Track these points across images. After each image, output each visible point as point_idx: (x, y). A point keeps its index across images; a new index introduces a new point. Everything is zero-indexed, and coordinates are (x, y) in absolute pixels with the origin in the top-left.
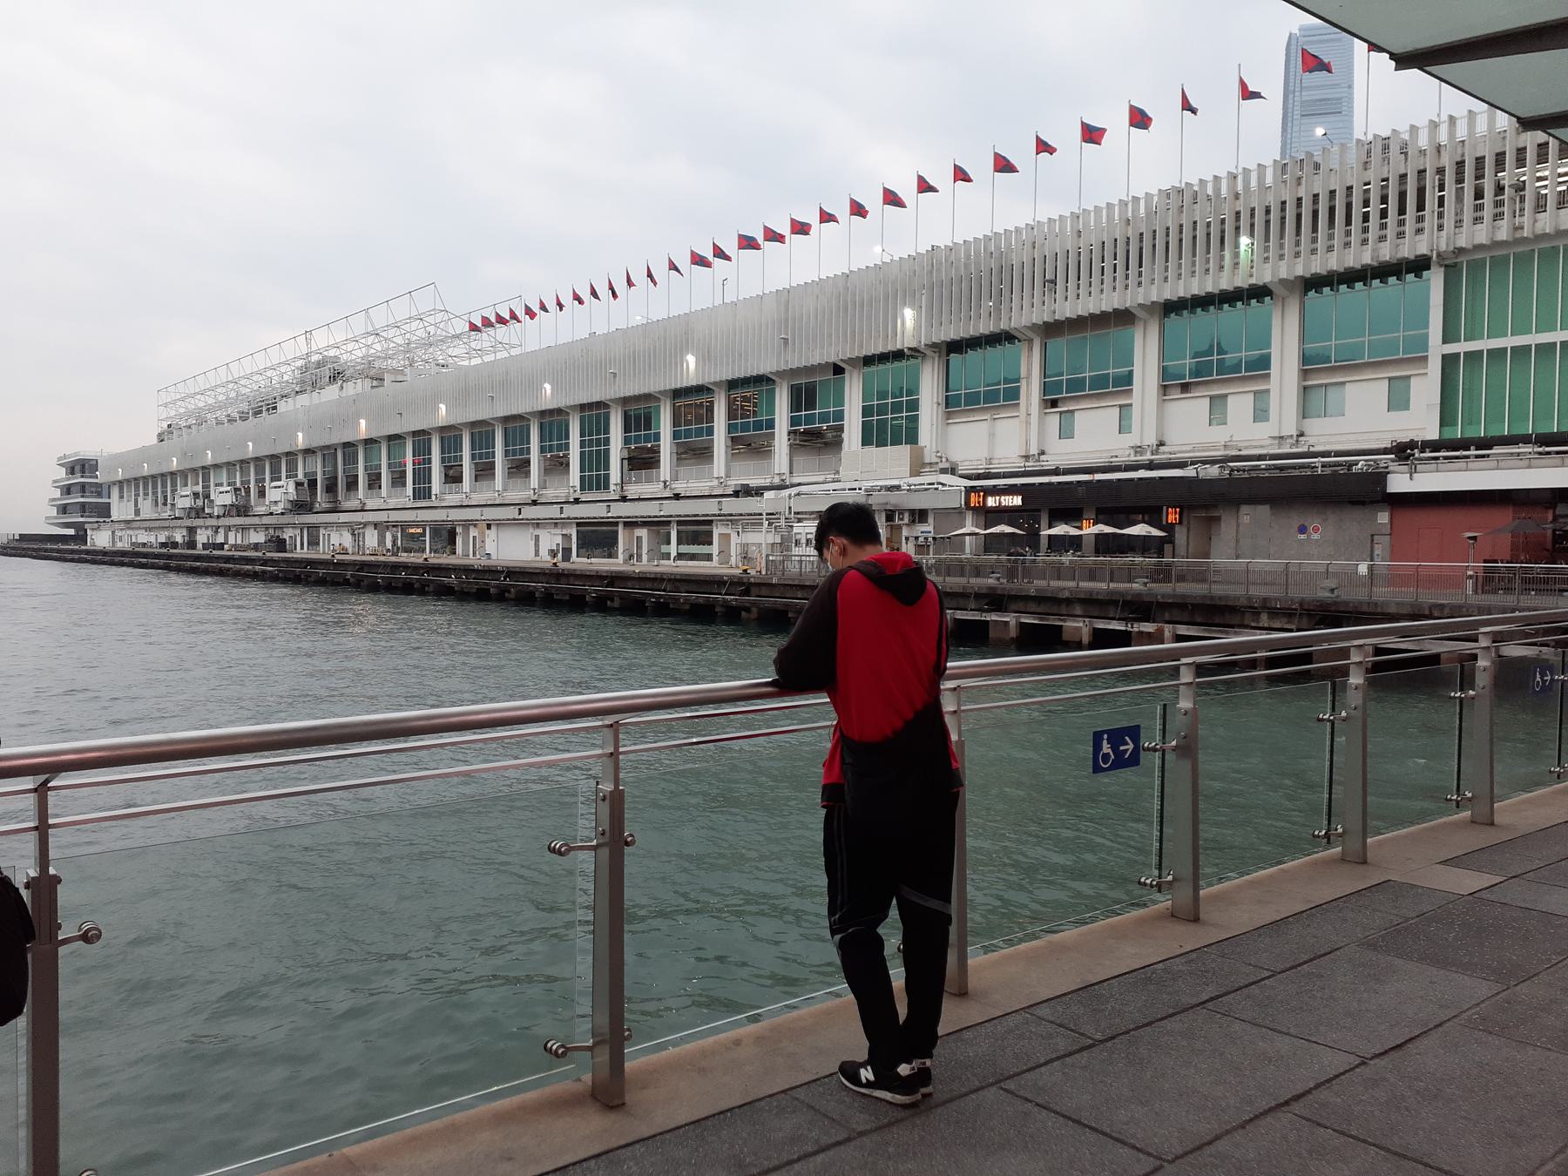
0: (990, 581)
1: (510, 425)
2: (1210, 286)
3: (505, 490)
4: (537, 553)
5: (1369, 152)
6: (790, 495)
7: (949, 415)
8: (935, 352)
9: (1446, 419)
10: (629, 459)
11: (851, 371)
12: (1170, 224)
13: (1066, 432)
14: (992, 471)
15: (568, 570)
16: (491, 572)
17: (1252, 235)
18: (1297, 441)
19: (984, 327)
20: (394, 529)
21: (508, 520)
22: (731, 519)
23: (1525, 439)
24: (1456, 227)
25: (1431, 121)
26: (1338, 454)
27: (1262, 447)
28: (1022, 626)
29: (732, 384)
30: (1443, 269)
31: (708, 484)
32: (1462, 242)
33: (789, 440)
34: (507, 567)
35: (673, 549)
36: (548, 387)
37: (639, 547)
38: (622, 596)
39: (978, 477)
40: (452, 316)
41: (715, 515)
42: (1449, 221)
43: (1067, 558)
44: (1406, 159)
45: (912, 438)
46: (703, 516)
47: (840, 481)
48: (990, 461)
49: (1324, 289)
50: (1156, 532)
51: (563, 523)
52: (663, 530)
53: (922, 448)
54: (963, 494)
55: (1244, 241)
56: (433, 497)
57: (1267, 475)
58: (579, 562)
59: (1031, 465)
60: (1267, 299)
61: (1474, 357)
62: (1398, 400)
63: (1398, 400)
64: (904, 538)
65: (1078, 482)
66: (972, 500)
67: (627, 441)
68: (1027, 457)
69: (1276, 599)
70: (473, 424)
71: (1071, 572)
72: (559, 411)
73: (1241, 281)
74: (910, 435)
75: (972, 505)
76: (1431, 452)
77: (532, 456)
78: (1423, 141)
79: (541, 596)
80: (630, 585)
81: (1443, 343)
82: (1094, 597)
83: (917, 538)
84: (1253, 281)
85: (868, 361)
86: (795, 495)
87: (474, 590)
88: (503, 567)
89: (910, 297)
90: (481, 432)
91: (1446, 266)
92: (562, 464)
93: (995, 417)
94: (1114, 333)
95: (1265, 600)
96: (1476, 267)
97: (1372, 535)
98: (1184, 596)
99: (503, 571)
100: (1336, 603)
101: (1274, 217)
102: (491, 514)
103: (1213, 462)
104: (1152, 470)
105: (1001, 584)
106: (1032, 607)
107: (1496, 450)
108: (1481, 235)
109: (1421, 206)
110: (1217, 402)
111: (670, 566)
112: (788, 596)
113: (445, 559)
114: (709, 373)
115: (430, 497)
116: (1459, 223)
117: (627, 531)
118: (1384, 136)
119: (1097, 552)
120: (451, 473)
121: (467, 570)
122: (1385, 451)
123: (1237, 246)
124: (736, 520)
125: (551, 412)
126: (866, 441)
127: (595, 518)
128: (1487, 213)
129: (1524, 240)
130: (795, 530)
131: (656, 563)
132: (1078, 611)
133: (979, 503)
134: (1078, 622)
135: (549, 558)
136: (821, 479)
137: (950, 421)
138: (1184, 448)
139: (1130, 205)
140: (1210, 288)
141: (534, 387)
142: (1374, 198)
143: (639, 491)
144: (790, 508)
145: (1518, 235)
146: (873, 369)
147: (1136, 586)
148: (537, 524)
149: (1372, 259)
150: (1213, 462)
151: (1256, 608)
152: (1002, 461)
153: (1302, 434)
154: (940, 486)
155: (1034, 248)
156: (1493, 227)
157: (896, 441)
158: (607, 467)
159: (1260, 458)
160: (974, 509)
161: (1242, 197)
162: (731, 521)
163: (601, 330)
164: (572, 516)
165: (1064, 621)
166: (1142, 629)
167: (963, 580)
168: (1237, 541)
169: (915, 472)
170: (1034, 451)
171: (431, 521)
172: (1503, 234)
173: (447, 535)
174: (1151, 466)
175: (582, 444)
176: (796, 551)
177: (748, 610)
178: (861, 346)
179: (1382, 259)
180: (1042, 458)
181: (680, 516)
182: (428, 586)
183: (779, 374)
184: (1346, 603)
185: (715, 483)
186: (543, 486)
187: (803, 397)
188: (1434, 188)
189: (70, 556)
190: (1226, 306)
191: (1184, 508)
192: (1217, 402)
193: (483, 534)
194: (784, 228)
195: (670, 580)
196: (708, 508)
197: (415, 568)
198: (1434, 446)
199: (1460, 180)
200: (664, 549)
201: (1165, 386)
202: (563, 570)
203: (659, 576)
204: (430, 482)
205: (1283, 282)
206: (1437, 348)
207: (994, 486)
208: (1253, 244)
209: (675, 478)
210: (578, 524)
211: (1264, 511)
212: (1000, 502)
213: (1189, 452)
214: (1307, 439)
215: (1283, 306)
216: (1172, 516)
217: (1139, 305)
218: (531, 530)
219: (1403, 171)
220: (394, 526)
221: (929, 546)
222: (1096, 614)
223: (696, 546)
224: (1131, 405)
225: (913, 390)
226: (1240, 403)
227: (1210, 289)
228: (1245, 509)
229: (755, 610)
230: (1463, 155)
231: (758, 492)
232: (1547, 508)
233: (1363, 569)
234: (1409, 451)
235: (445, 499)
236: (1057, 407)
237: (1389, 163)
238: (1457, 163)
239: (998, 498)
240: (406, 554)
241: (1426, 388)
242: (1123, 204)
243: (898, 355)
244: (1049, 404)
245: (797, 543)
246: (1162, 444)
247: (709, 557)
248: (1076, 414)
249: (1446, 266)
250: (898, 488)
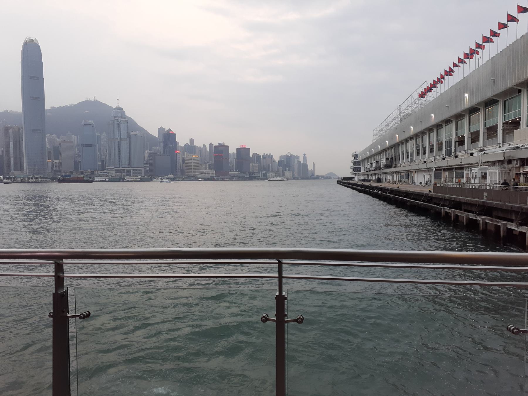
189: (343, 184)
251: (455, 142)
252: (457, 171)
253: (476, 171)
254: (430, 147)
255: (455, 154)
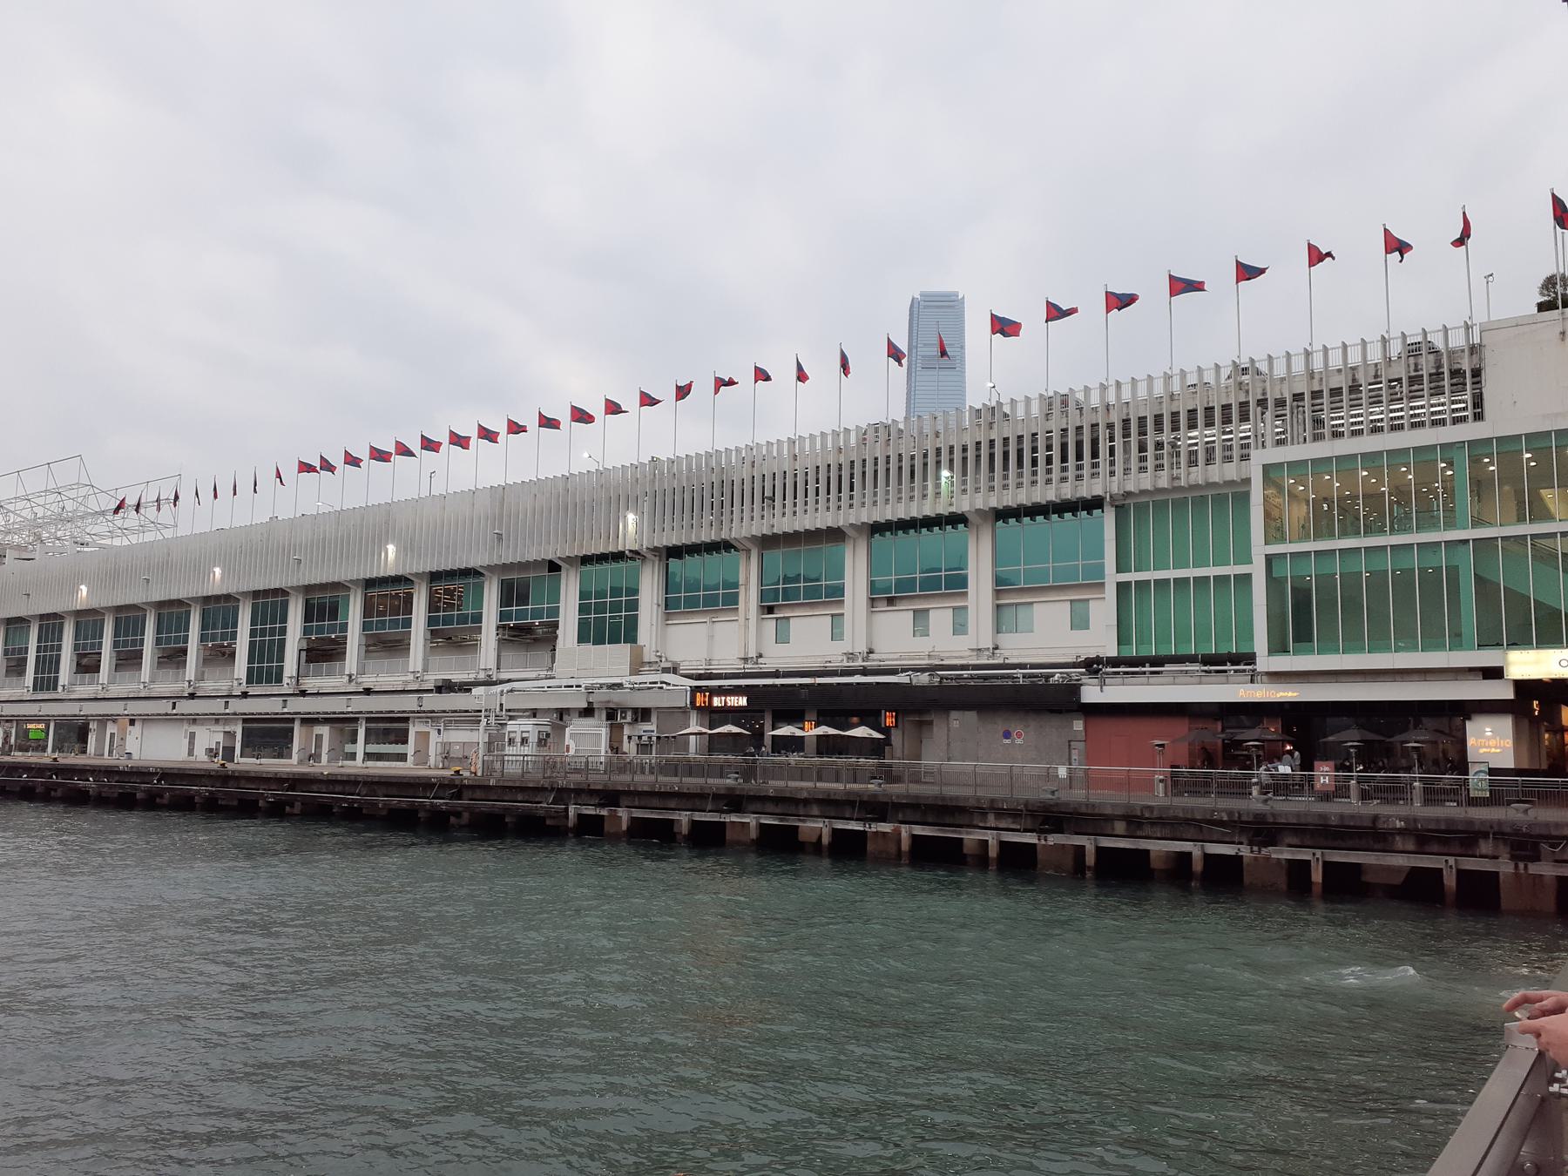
0: (728, 781)
1: (165, 611)
2: (915, 511)
3: (152, 681)
4: (191, 752)
5: (1050, 404)
6: (502, 691)
7: (668, 616)
8: (655, 556)
9: (1122, 639)
10: (308, 650)
11: (568, 570)
12: (878, 455)
13: (782, 637)
14: (714, 671)
15: (240, 772)
16: (141, 774)
17: (951, 469)
18: (993, 653)
19: (706, 535)
20: (7, 724)
21: (159, 715)
22: (431, 716)
23: (1192, 659)
24: (1124, 474)
25: (1102, 384)
26: (1033, 666)
27: (961, 657)
28: (762, 827)
29: (435, 577)
30: (1114, 509)
31: (404, 678)
32: (1131, 487)
33: (497, 634)
34: (161, 768)
35: (360, 748)
36: (218, 571)
37: (319, 746)
38: (306, 802)
39: (699, 677)
40: (96, 491)
41: (413, 712)
42: (1119, 468)
43: (794, 758)
44: (1081, 414)
45: (631, 637)
46: (399, 712)
47: (554, 678)
48: (709, 662)
49: (1010, 520)
50: (876, 735)
51: (226, 719)
52: (348, 727)
53: (642, 648)
54: (689, 693)
55: (945, 473)
56: (60, 689)
57: (972, 684)
58: (244, 763)
59: (749, 666)
60: (961, 526)
61: (1142, 585)
62: (1080, 621)
63: (1080, 621)
64: (625, 738)
65: (801, 685)
66: (698, 699)
67: (306, 631)
68: (745, 660)
69: (1003, 800)
70: (119, 609)
71: (802, 773)
72: (228, 597)
73: (943, 509)
74: (626, 632)
75: (698, 705)
76: (1151, 667)
77: (189, 645)
78: (1095, 400)
79: (201, 801)
80: (315, 788)
81: (1117, 572)
82: (832, 797)
83: (640, 737)
84: (953, 509)
85: (586, 560)
86: (508, 692)
87: (116, 795)
88: (156, 769)
89: (632, 502)
90: (128, 619)
91: (1116, 507)
92: (224, 654)
93: (714, 620)
94: (827, 549)
95: (993, 801)
96: (1141, 509)
97: (1069, 741)
98: (917, 797)
99: (157, 773)
100: (1057, 805)
101: (971, 454)
102: (135, 708)
103: (923, 670)
104: (866, 675)
105: (739, 784)
106: (770, 807)
107: (1167, 668)
108: (1146, 481)
109: (1095, 454)
110: (920, 616)
111: (358, 766)
112: (506, 798)
113: (71, 759)
114: (411, 564)
115: (55, 688)
116: (1127, 471)
117: (304, 729)
118: (1063, 392)
119: (820, 753)
120: (84, 661)
121: (110, 772)
122: (1074, 665)
123: (938, 478)
124: (438, 717)
125: (217, 598)
126: (583, 638)
127: (268, 714)
128: (1150, 463)
129: (1181, 489)
130: (509, 728)
131: (340, 764)
132: (815, 810)
133: (705, 702)
134: (817, 822)
135: (206, 758)
136: (533, 675)
137: (670, 622)
138: (891, 656)
139: (842, 435)
140: (915, 513)
141: (203, 572)
142: (1041, 445)
143: (319, 685)
144: (501, 705)
145: (1176, 484)
146: (589, 567)
147: (872, 787)
148: (194, 719)
149: (1056, 496)
150: (923, 670)
151: (983, 809)
152: (721, 662)
153: (996, 648)
154: (664, 686)
155: (753, 466)
156: (1156, 476)
157: (614, 640)
158: (281, 659)
159: (963, 667)
160: (700, 709)
161: (942, 436)
162: (431, 718)
163: (285, 514)
164: (238, 712)
165: (803, 821)
166: (880, 829)
167: (701, 781)
168: (949, 744)
169: (635, 671)
170: (752, 654)
171: (59, 716)
172: (1164, 482)
173: (76, 732)
174: (865, 672)
175: (253, 633)
176: (509, 750)
177: (458, 815)
178: (581, 546)
179: (1064, 497)
180: (760, 660)
181: (372, 712)
182: (55, 790)
183: (491, 568)
184: (1067, 804)
185: (411, 677)
186: (200, 677)
187: (513, 593)
188: (1105, 440)
190: (900, 532)
191: (900, 712)
192: (920, 616)
193: (124, 731)
194: (500, 427)
195: (365, 783)
196: (408, 703)
197: (40, 770)
198: (1114, 662)
199: (1126, 435)
200: (349, 748)
201: (873, 599)
202: (233, 772)
203: (353, 778)
204: (57, 671)
205: (978, 511)
206: (1112, 577)
207: (720, 686)
208: (952, 477)
209: (361, 672)
210: (245, 721)
211: (971, 716)
212: (725, 702)
213: (896, 660)
214: (1002, 651)
215: (977, 531)
216: (889, 720)
217: (851, 525)
218: (186, 726)
219: (1079, 424)
220: (7, 721)
221: (651, 745)
222: (833, 814)
223: (387, 745)
224: (843, 614)
225: (634, 591)
226: (940, 616)
227: (915, 514)
228: (954, 714)
229: (466, 815)
230: (1128, 414)
231: (465, 688)
232: (1216, 720)
233: (1062, 772)
234: (1095, 666)
235: (74, 691)
236: (772, 613)
237: (1067, 417)
238: (1124, 421)
239: (723, 698)
240: (20, 753)
241: (1104, 610)
242: (836, 434)
243: (618, 556)
244: (766, 611)
245: (511, 741)
246: (871, 652)
247: (402, 757)
248: (791, 620)
249: (1116, 507)
250: (620, 686)
251: (300, 650)
252: (368, 725)
253: (529, 728)
254: (156, 651)
255: (298, 680)
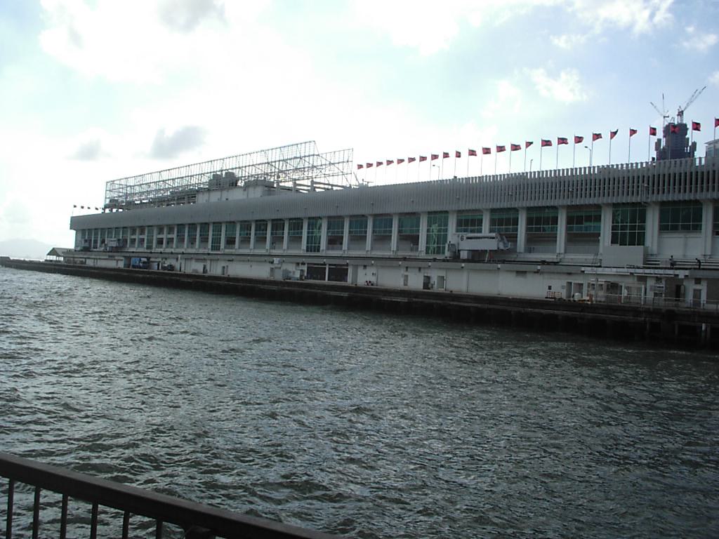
74: (637, 238)
126: (614, 241)
157: (632, 244)
